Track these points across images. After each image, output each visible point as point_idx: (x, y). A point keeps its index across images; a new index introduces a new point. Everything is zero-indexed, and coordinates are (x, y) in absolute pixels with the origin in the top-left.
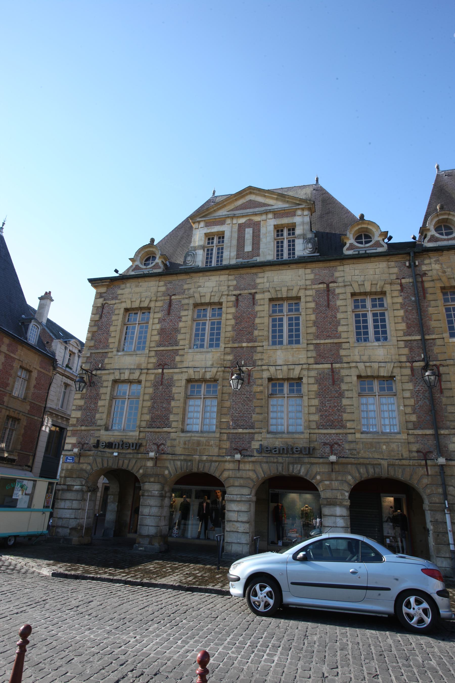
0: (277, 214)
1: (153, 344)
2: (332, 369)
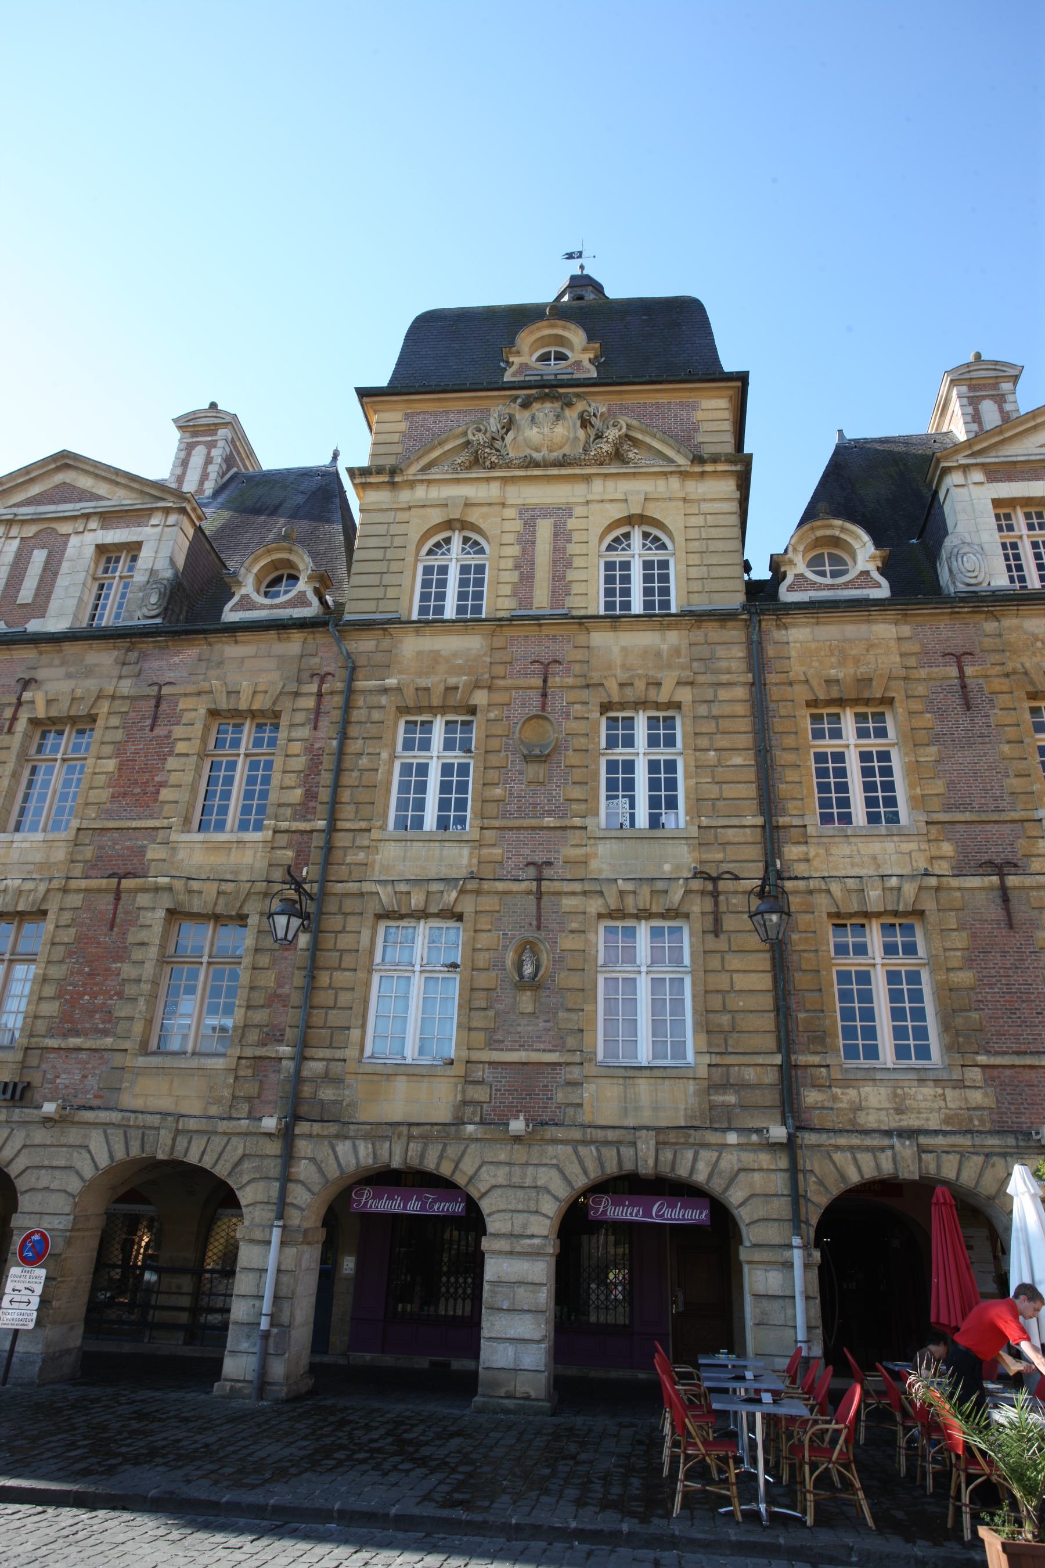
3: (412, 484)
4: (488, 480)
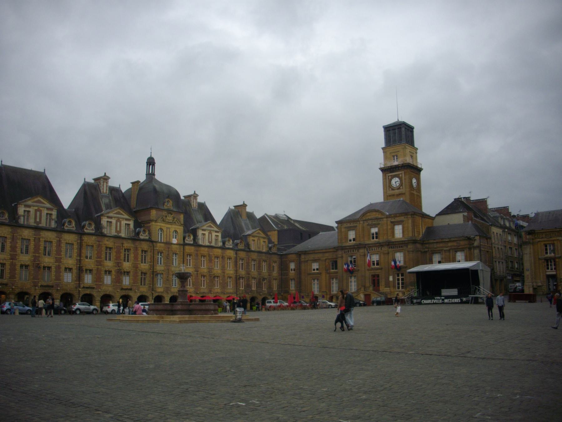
0: (48, 209)
1: (9, 251)
2: (59, 265)
3: (157, 222)
4: (164, 223)
